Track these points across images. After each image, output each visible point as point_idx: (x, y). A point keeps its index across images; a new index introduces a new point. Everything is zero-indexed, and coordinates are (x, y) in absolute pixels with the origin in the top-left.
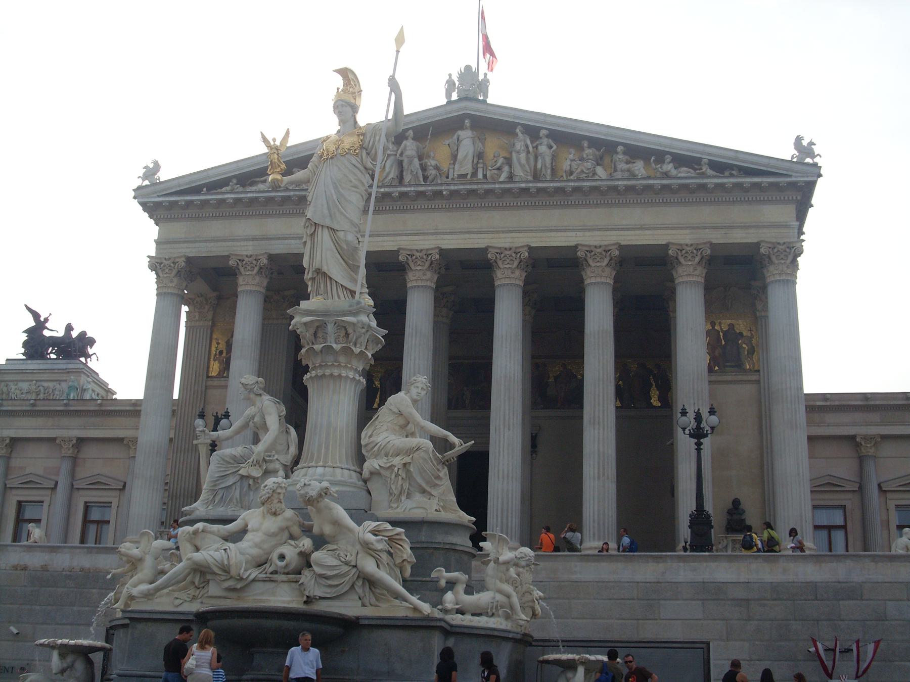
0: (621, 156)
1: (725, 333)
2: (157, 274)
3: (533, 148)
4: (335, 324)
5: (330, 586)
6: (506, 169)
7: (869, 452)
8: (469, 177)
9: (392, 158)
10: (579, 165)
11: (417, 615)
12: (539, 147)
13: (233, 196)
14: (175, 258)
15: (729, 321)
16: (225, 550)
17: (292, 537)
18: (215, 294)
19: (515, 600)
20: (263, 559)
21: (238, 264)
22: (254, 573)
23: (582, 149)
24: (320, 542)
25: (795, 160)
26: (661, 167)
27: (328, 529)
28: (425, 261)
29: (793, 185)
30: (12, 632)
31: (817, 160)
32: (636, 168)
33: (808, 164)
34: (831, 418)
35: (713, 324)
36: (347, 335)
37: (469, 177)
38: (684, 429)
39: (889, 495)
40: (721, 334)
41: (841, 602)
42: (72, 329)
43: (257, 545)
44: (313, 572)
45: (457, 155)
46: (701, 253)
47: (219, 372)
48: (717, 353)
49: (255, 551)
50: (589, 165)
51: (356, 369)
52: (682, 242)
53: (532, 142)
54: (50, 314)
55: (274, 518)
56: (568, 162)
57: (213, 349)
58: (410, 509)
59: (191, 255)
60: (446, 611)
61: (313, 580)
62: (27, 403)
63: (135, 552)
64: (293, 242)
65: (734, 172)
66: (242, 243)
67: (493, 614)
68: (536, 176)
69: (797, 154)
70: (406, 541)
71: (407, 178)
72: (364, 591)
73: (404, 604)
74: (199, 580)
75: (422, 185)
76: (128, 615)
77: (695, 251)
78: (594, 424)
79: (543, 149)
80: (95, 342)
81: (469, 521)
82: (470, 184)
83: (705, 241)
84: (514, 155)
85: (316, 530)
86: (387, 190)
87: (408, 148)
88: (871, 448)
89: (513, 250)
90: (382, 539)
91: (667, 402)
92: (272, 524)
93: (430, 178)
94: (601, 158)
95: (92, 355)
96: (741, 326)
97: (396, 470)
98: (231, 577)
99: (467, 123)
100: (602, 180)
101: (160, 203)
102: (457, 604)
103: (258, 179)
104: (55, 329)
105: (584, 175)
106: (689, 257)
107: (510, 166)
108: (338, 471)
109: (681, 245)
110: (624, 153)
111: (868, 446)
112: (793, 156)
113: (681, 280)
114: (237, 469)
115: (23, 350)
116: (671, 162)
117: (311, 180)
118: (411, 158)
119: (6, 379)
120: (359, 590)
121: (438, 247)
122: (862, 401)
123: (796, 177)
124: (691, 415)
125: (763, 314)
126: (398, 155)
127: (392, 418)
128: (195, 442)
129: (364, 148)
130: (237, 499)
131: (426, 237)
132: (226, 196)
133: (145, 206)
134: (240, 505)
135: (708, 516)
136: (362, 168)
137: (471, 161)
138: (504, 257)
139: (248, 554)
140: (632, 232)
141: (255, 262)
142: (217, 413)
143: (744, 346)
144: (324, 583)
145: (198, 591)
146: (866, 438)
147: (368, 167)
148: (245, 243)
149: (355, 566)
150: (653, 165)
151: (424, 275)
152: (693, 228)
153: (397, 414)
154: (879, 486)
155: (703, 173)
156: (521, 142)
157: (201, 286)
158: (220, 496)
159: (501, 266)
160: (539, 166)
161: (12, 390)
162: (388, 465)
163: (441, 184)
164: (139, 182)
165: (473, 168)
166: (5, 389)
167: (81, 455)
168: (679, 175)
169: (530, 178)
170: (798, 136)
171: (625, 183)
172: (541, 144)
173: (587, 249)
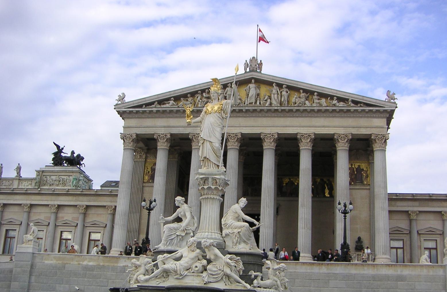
0: (316, 97)
1: (357, 169)
2: (124, 141)
3: (280, 92)
4: (212, 178)
5: (214, 278)
6: (269, 100)
7: (413, 218)
8: (253, 104)
9: (222, 95)
10: (299, 100)
12: (283, 92)
13: (156, 109)
14: (131, 134)
15: (358, 164)
16: (175, 264)
17: (199, 260)
18: (146, 148)
19: (279, 282)
20: (189, 268)
21: (158, 137)
22: (186, 273)
23: (300, 93)
24: (209, 262)
25: (387, 101)
26: (332, 102)
27: (212, 257)
28: (235, 138)
29: (385, 111)
30: (76, 289)
31: (396, 101)
32: (322, 102)
33: (392, 103)
34: (399, 203)
35: (352, 165)
36: (216, 182)
37: (253, 104)
38: (339, 210)
39: (421, 235)
40: (355, 169)
41: (398, 282)
42: (74, 153)
43: (187, 263)
44: (207, 273)
45: (249, 94)
46: (348, 137)
47: (148, 180)
48: (353, 177)
49: (186, 265)
50: (303, 100)
51: (220, 195)
52: (340, 133)
53: (280, 90)
54: (64, 146)
55: (193, 252)
56: (294, 98)
57: (145, 170)
58: (240, 249)
59: (138, 133)
60: (254, 287)
61: (207, 276)
62: (65, 190)
63: (138, 263)
64: (180, 128)
65: (362, 105)
66: (159, 129)
67: (271, 288)
68: (281, 104)
69: (388, 98)
70: (240, 261)
72: (226, 280)
73: (240, 284)
74: (166, 275)
76: (139, 287)
77: (345, 137)
78: (303, 206)
79: (284, 93)
80: (84, 158)
81: (262, 253)
82: (254, 107)
83: (349, 133)
84: (272, 95)
85: (208, 257)
87: (228, 91)
88: (415, 216)
89: (271, 134)
90: (233, 262)
91: (332, 195)
94: (308, 97)
95: (82, 164)
96: (363, 166)
97: (235, 234)
98: (178, 274)
99: (253, 81)
100: (308, 107)
101: (126, 111)
102: (258, 284)
103: (166, 102)
104: (67, 153)
105: (301, 105)
106: (343, 139)
107: (271, 99)
108: (213, 234)
109: (340, 134)
110: (317, 95)
111: (414, 215)
112: (386, 99)
114: (175, 232)
115: (52, 162)
117: (202, 121)
118: (229, 95)
119: (46, 174)
120: (224, 279)
121: (241, 132)
122: (411, 196)
123: (387, 108)
124: (342, 205)
125: (372, 161)
126: (224, 94)
127: (233, 214)
128: (159, 222)
129: (222, 110)
130: (175, 244)
131: (236, 128)
132: (153, 109)
133: (119, 112)
134: (176, 246)
135: (348, 245)
136: (222, 118)
137: (254, 97)
138: (268, 137)
139: (183, 266)
140: (319, 128)
141: (165, 137)
142: (151, 200)
143: (364, 174)
145: (165, 279)
146: (412, 212)
147: (224, 117)
148: (161, 128)
149: (222, 271)
150: (329, 101)
151: (235, 143)
152: (344, 127)
154: (418, 232)
155: (349, 105)
156: (275, 89)
157: (141, 145)
158: (169, 242)
159: (266, 141)
160: (282, 100)
161: (48, 179)
163: (242, 107)
164: (117, 102)
165: (255, 100)
166: (45, 179)
167: (87, 213)
168: (339, 106)
169: (279, 105)
170: (388, 91)
171: (317, 108)
172: (283, 91)
173: (302, 135)
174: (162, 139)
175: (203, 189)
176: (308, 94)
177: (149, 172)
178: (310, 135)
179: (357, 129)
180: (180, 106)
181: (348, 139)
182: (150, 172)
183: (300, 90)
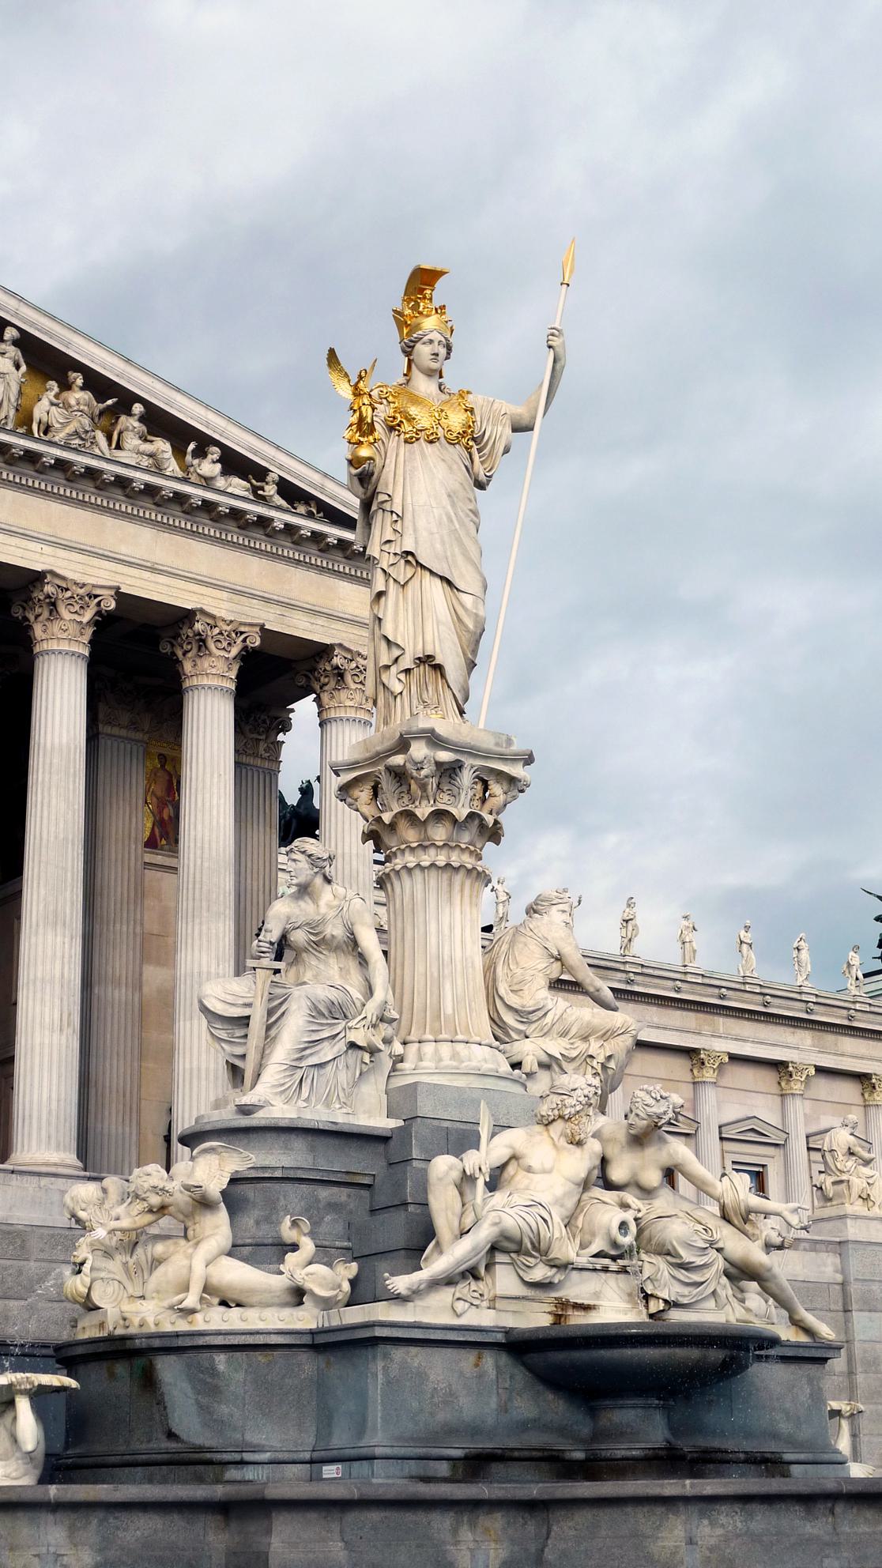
0: (137, 424)
11: (803, 1339)
23: (66, 386)
26: (199, 465)
46: (244, 640)
55: (577, 1151)
77: (234, 635)
105: (77, 441)
106: (225, 644)
110: (142, 419)
113: (205, 681)
116: (218, 461)
144: (682, 1278)
153: (553, 957)
162: (574, 1054)
168: (229, 490)
175: (440, 815)
176: (110, 402)
178: (98, 592)
179: (279, 610)
181: (245, 648)
183: (75, 375)
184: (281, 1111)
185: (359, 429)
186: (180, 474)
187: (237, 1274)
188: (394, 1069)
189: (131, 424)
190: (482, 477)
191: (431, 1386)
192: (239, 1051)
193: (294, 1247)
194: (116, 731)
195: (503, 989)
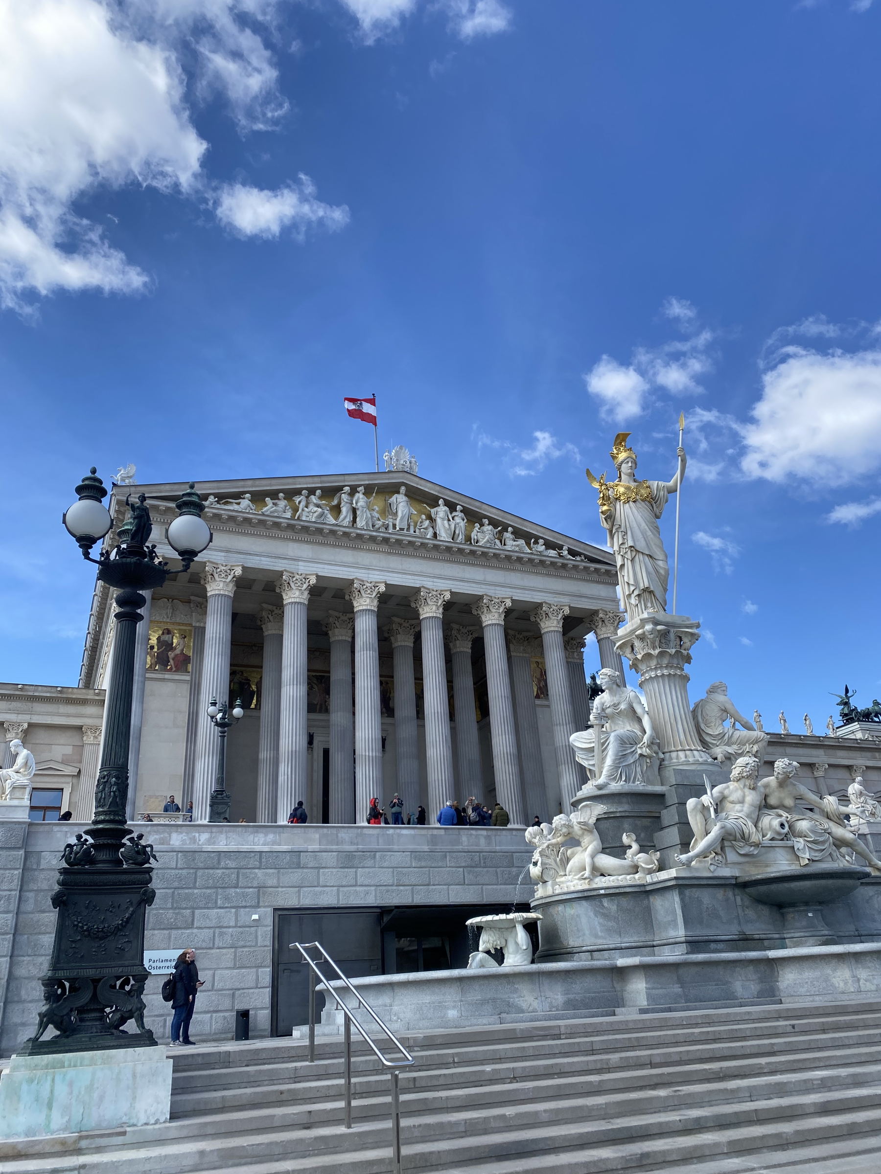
12: (456, 518)
23: (482, 525)
47: (151, 665)
53: (451, 514)
55: (753, 792)
71: (360, 523)
75: (373, 531)
79: (458, 520)
84: (439, 521)
86: (347, 530)
92: (751, 798)
93: (377, 526)
99: (403, 489)
110: (512, 533)
156: (441, 511)
160: (457, 532)
162: (740, 751)
174: (223, 575)
176: (499, 528)
177: (152, 647)
180: (266, 513)
182: (156, 647)
184: (615, 787)
185: (603, 499)
186: (529, 551)
187: (607, 861)
188: (661, 765)
189: (508, 535)
190: (658, 514)
191: (705, 906)
192: (591, 762)
193: (630, 847)
194: (518, 654)
195: (703, 726)
